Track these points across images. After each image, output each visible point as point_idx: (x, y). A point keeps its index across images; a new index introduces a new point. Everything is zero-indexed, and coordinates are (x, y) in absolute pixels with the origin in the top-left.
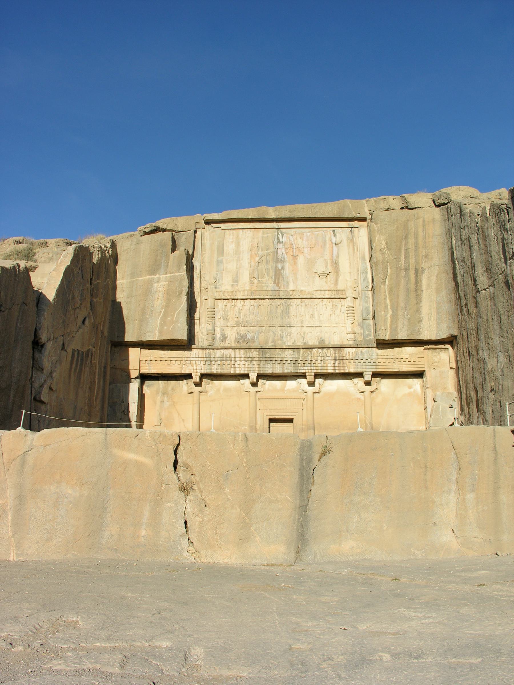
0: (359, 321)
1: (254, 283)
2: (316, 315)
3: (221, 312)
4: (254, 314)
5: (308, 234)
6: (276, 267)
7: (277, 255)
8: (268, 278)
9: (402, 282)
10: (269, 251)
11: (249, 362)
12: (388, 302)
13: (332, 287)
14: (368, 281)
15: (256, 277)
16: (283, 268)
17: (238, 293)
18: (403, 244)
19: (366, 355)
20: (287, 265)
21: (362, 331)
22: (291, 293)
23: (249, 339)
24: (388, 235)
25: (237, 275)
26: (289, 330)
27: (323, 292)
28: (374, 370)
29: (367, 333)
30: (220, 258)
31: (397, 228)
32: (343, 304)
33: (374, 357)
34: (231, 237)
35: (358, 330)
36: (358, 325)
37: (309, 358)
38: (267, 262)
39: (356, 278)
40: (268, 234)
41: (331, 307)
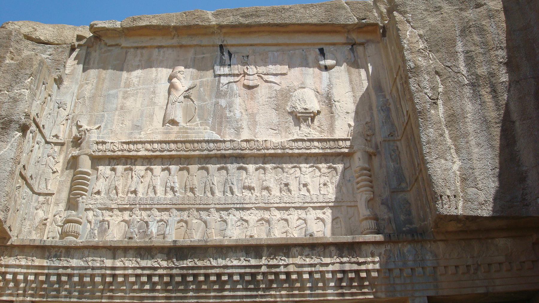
0: (384, 197)
1: (172, 129)
2: (294, 186)
3: (102, 180)
4: (169, 185)
5: (276, 54)
6: (217, 103)
7: (218, 86)
8: (199, 122)
9: (469, 107)
10: (204, 79)
11: (144, 279)
12: (449, 141)
13: (325, 136)
14: (393, 125)
15: (178, 119)
16: (230, 106)
17: (140, 146)
18: (460, 44)
19: (411, 258)
20: (238, 101)
21: (391, 215)
22: (244, 144)
23: (152, 232)
24: (428, 28)
25: (141, 116)
26: (239, 214)
27: (308, 144)
28: (431, 293)
29: (402, 217)
30: (112, 92)
31: (444, 20)
32: (348, 165)
33: (429, 264)
34: (138, 59)
35: (384, 213)
36: (382, 204)
37: (282, 269)
38: (200, 98)
39: (368, 120)
40: (203, 54)
41: (324, 170)
